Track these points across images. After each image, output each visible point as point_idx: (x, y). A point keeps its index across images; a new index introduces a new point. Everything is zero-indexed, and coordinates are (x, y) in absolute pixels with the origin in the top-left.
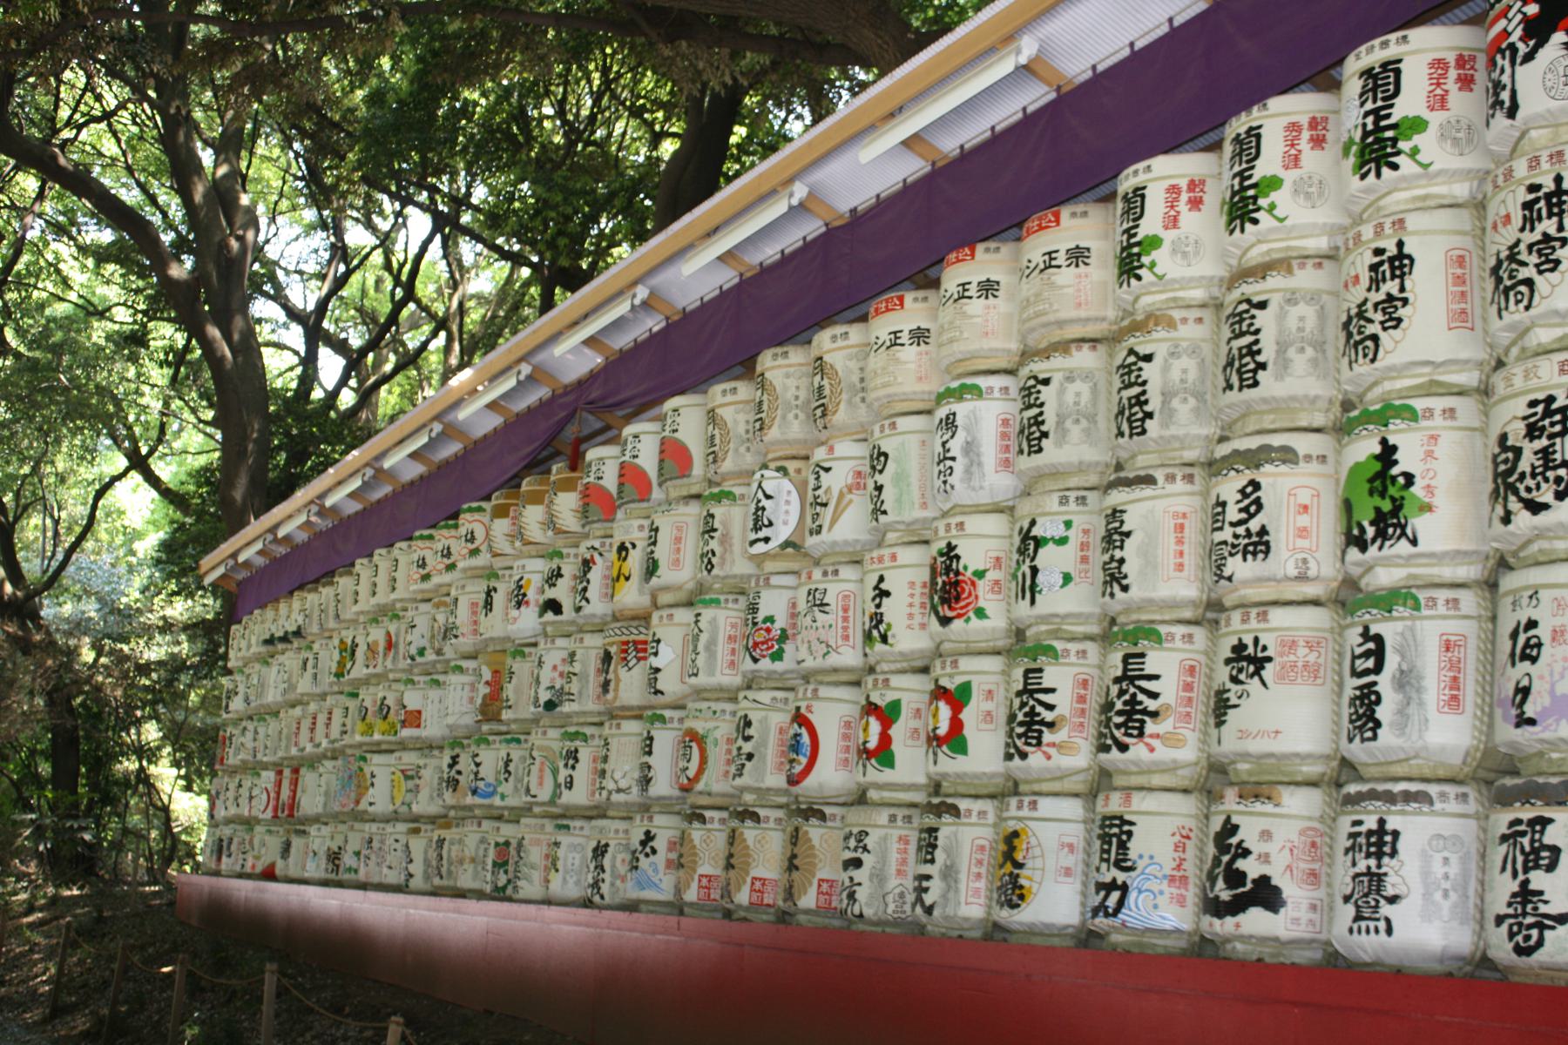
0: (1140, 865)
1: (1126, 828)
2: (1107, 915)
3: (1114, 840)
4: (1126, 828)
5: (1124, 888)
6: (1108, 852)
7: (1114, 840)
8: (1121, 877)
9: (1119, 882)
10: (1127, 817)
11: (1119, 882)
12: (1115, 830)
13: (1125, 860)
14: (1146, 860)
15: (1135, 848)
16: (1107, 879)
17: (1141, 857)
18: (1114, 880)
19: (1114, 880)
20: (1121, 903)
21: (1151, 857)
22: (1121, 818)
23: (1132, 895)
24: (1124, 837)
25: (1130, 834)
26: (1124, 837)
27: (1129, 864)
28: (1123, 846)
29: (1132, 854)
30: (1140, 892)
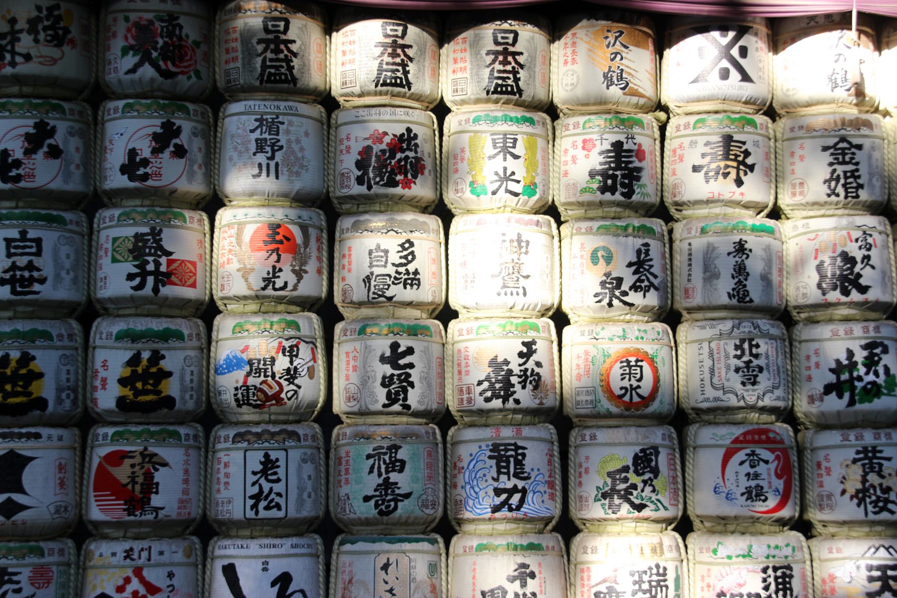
0: (533, 475)
1: (520, 451)
2: (510, 509)
3: (512, 460)
4: (520, 451)
5: (524, 491)
6: (508, 467)
7: (512, 460)
8: (520, 484)
9: (520, 487)
10: (520, 443)
11: (520, 487)
12: (513, 453)
13: (523, 473)
14: (536, 472)
15: (528, 464)
16: (509, 485)
17: (532, 470)
18: (515, 486)
19: (515, 486)
20: (522, 501)
21: (538, 470)
22: (515, 444)
23: (530, 496)
24: (520, 457)
25: (524, 455)
26: (520, 457)
27: (526, 475)
28: (519, 463)
29: (527, 469)
30: (534, 493)
